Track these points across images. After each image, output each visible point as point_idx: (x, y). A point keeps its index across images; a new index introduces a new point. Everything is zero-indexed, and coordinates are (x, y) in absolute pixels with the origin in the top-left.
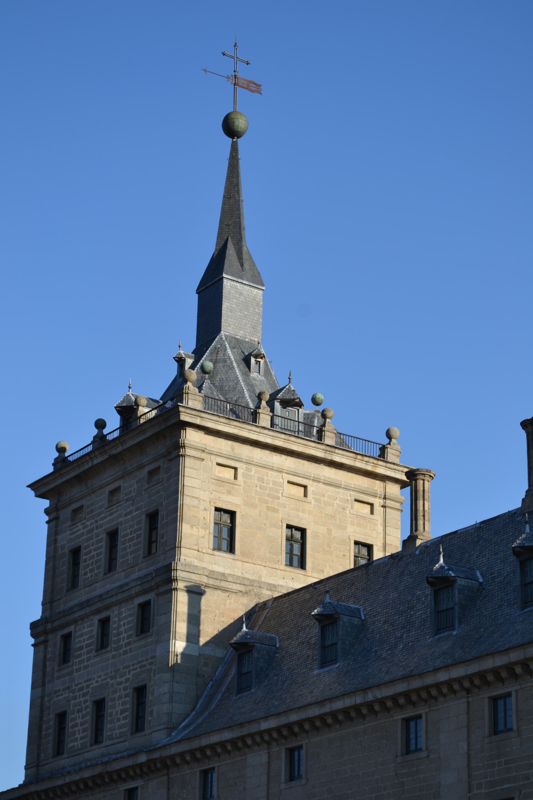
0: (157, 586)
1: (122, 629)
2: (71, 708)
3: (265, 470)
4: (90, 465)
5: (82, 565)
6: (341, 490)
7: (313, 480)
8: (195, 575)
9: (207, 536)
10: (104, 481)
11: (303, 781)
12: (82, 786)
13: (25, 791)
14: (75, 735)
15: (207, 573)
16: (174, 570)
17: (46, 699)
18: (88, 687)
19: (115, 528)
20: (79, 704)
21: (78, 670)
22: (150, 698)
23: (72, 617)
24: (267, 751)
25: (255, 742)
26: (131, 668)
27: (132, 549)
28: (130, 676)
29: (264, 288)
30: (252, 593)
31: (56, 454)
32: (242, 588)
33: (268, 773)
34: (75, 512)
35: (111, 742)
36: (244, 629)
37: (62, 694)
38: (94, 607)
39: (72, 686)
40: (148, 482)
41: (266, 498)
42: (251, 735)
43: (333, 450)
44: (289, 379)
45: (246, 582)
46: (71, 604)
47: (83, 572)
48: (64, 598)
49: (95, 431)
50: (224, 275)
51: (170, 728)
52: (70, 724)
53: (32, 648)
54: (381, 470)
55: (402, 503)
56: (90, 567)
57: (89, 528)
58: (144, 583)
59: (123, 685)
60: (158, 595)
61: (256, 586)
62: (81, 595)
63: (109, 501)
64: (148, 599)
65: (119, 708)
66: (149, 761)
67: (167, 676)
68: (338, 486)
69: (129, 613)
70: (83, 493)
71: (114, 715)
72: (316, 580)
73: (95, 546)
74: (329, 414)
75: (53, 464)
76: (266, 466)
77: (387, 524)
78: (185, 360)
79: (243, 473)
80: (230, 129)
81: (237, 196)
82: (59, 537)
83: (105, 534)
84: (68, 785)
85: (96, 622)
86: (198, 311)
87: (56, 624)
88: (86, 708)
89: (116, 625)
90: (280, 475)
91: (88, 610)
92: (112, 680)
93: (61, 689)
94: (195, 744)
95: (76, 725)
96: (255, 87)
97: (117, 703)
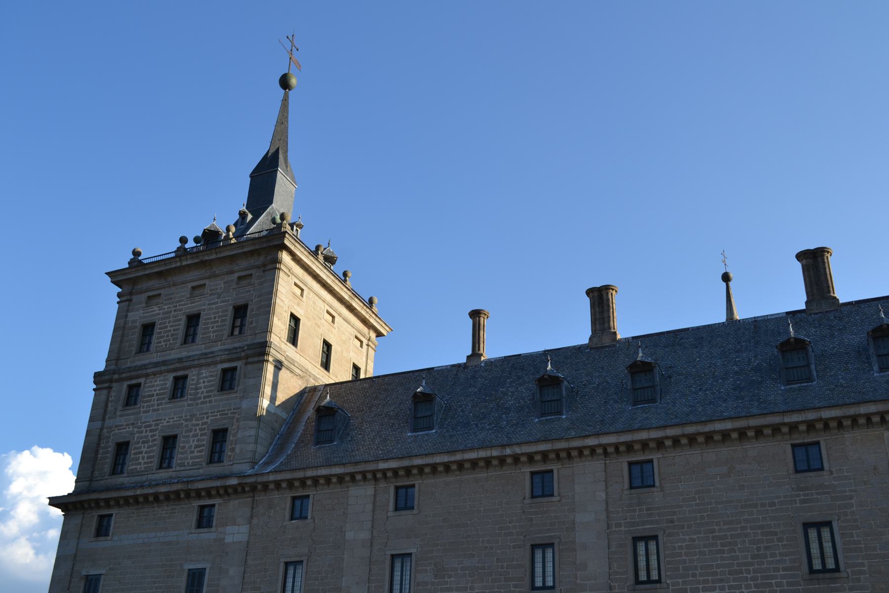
0: (247, 357)
1: (202, 385)
4: (178, 264)
5: (155, 336)
11: (415, 511)
12: (151, 499)
13: (74, 499)
17: (105, 430)
18: (157, 425)
20: (146, 437)
21: (144, 412)
22: (230, 438)
23: (144, 372)
25: (365, 478)
28: (209, 421)
32: (300, 373)
33: (374, 503)
34: (149, 298)
35: (183, 468)
38: (170, 367)
40: (237, 284)
42: (364, 474)
49: (179, 245)
52: (133, 452)
54: (372, 321)
63: (191, 294)
65: (193, 443)
66: (239, 484)
67: (255, 423)
68: (349, 323)
74: (350, 274)
75: (129, 263)
80: (285, 82)
84: (136, 498)
85: (172, 378)
87: (124, 375)
88: (154, 440)
91: (163, 368)
94: (300, 474)
95: (141, 453)
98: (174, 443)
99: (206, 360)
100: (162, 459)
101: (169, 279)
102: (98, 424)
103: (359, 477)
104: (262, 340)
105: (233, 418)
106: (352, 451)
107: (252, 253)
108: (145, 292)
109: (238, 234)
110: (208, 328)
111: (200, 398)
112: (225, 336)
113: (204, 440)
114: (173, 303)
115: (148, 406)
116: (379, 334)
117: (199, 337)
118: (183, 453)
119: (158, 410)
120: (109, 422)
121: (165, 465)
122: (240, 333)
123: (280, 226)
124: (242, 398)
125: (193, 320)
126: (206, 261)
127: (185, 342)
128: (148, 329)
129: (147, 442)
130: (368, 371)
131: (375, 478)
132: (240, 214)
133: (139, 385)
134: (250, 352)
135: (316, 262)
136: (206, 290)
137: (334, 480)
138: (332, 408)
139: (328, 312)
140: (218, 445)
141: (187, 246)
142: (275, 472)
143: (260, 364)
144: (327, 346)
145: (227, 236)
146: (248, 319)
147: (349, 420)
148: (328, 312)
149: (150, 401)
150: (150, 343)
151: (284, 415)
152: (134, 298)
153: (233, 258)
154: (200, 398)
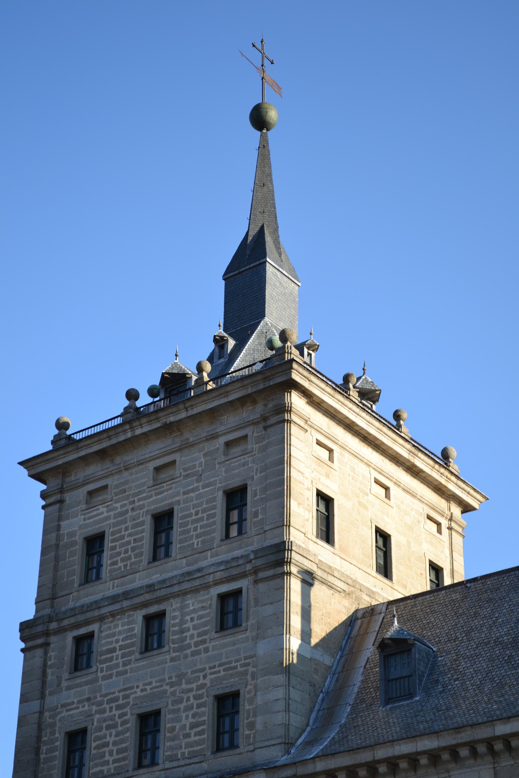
2: (95, 724)
3: (356, 460)
4: (129, 435)
6: (416, 501)
7: (395, 483)
8: (307, 561)
9: (311, 520)
10: (147, 456)
14: (104, 756)
15: (317, 562)
16: (288, 550)
17: (47, 714)
19: (241, 484)
20: (112, 718)
21: (104, 678)
22: (245, 706)
23: (97, 613)
24: (492, 766)
25: (474, 754)
26: (208, 671)
27: (199, 531)
28: (207, 681)
29: (300, 284)
30: (354, 596)
31: (56, 432)
34: (91, 493)
35: (175, 764)
36: (396, 623)
37: (78, 708)
38: (137, 600)
39: (96, 697)
40: (226, 454)
41: (358, 491)
42: (472, 746)
43: (416, 452)
44: (364, 369)
45: (350, 582)
46: (87, 600)
47: (109, 562)
48: (74, 594)
49: (126, 403)
50: (268, 259)
51: (288, 744)
52: (94, 745)
53: (22, 655)
54: (451, 487)
55: (463, 528)
56: (123, 555)
57: (119, 510)
58: (232, 567)
59: (194, 693)
60: (256, 582)
61: (357, 589)
62: (105, 588)
63: (154, 480)
64: (239, 586)
67: (281, 679)
68: (413, 495)
69: (200, 605)
70: (110, 470)
71: (177, 730)
72: (401, 596)
73: (130, 531)
74: (404, 415)
75: (53, 442)
76: (358, 455)
77: (453, 549)
78: (227, 340)
79: (338, 457)
80: (259, 120)
81: (270, 186)
82: (63, 524)
83: (149, 517)
85: (140, 619)
86: (225, 298)
87: (66, 622)
89: (177, 621)
90: (368, 469)
91: (126, 604)
92: (171, 687)
93: (75, 701)
95: (107, 745)
96: (278, 89)
97: (184, 715)
98: (157, 723)
99: (192, 583)
100: (141, 751)
101: (118, 460)
102: (35, 705)
103: (464, 752)
104: (277, 541)
105: (246, 673)
106: (447, 709)
107: (242, 401)
108: (83, 485)
109: (216, 374)
110: (189, 531)
111: (189, 646)
112: (217, 541)
113: (203, 714)
114: (127, 497)
115: (109, 668)
116: (466, 508)
117: (175, 548)
118: (172, 739)
119: (126, 672)
120: (51, 701)
121: (147, 761)
122: (240, 532)
123: (281, 352)
124: (256, 639)
125: (163, 520)
126: (171, 423)
127: (155, 558)
128: (95, 543)
129: (115, 726)
130: (456, 572)
131: (492, 752)
132: (215, 340)
133: (90, 636)
134: (259, 562)
135: (347, 402)
136: (178, 471)
137: (424, 761)
138: (405, 640)
139: (377, 482)
140: (227, 720)
141: (139, 403)
142: (324, 755)
143: (279, 580)
144: (383, 538)
145: (200, 382)
146: (250, 509)
147: (436, 657)
148: (377, 482)
149: (111, 659)
150: (100, 565)
151: (328, 660)
152: (68, 497)
153: (212, 414)
154: (189, 646)
